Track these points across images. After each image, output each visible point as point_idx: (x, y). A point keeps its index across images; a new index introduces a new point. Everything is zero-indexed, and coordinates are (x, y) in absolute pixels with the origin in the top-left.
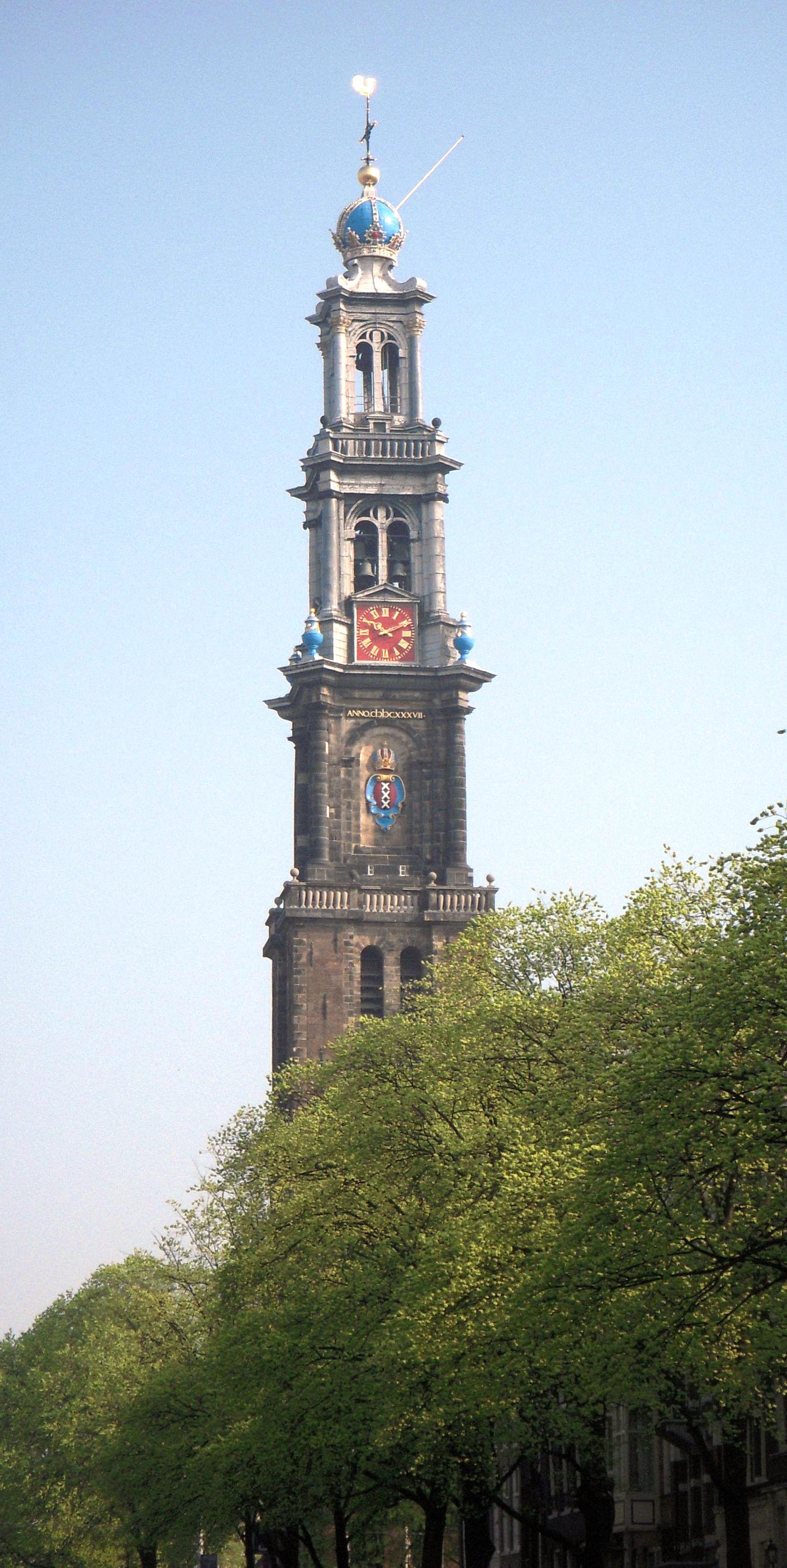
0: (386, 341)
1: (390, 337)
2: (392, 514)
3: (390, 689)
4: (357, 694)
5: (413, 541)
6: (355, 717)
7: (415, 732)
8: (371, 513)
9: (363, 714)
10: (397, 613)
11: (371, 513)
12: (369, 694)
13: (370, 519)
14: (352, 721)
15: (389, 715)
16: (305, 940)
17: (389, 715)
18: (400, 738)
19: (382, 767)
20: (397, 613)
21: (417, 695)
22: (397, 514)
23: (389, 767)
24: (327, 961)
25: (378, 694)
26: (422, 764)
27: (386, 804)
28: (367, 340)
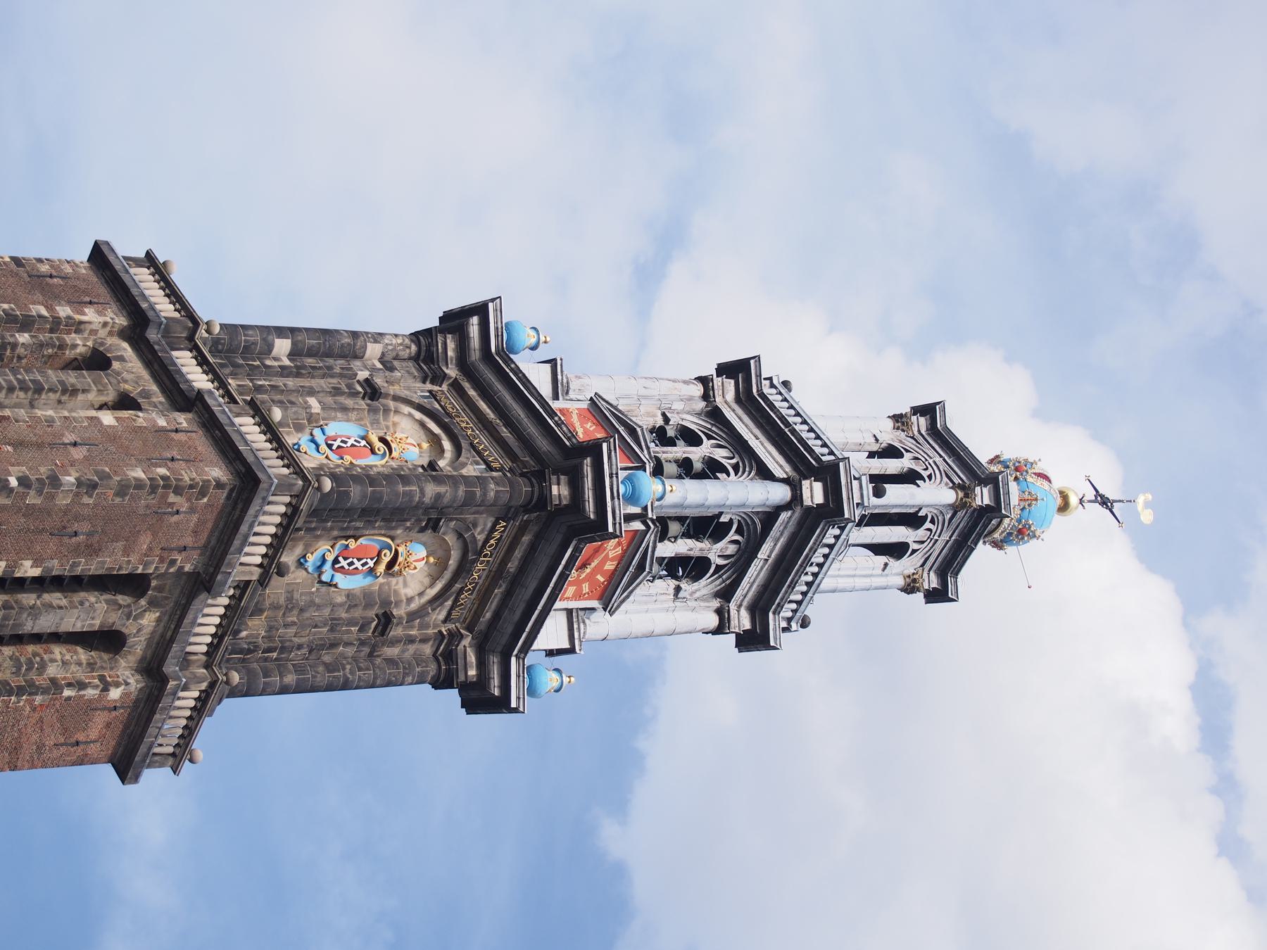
0: (914, 546)
1: (914, 551)
2: (721, 562)
3: (516, 581)
4: (526, 539)
5: (678, 589)
6: (493, 530)
7: (433, 610)
8: (737, 537)
9: (492, 542)
10: (602, 579)
11: (737, 537)
12: (518, 554)
13: (732, 535)
14: (489, 525)
15: (475, 575)
16: (205, 500)
17: (475, 575)
18: (432, 585)
19: (400, 559)
20: (602, 579)
21: (488, 615)
22: (719, 568)
23: (396, 568)
24: (155, 534)
25: (512, 566)
26: (386, 620)
27: (344, 563)
28: (928, 525)
